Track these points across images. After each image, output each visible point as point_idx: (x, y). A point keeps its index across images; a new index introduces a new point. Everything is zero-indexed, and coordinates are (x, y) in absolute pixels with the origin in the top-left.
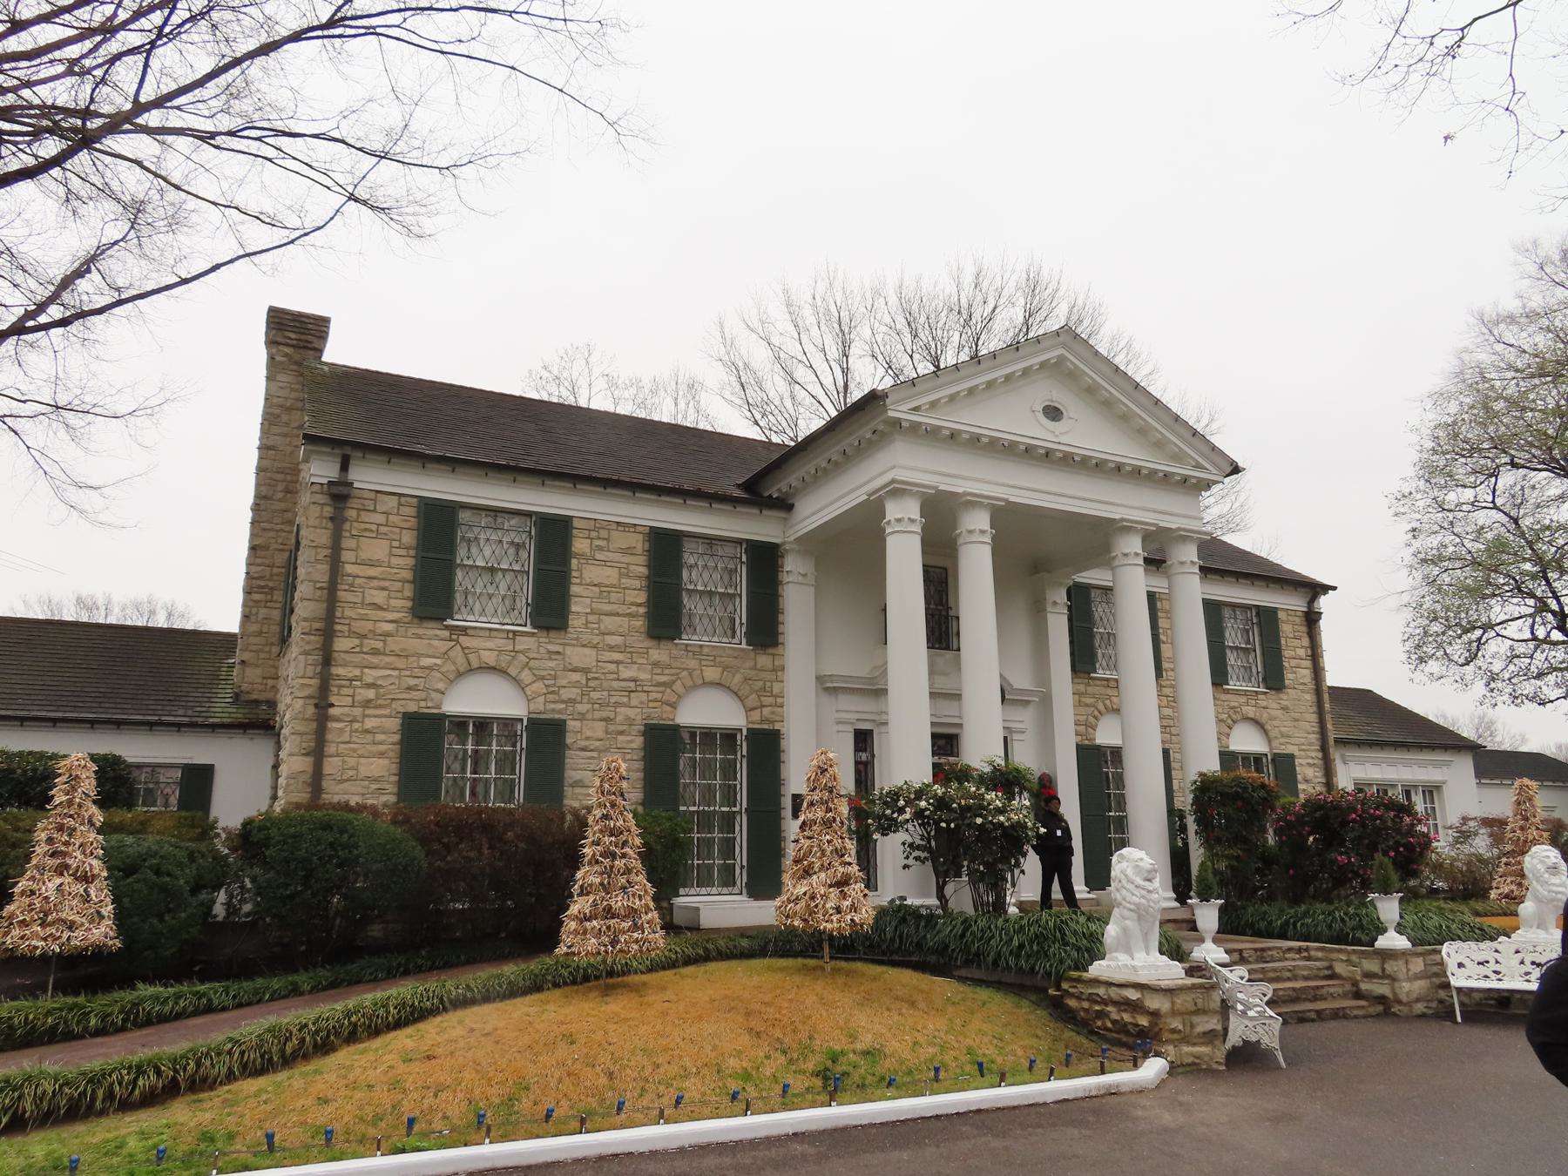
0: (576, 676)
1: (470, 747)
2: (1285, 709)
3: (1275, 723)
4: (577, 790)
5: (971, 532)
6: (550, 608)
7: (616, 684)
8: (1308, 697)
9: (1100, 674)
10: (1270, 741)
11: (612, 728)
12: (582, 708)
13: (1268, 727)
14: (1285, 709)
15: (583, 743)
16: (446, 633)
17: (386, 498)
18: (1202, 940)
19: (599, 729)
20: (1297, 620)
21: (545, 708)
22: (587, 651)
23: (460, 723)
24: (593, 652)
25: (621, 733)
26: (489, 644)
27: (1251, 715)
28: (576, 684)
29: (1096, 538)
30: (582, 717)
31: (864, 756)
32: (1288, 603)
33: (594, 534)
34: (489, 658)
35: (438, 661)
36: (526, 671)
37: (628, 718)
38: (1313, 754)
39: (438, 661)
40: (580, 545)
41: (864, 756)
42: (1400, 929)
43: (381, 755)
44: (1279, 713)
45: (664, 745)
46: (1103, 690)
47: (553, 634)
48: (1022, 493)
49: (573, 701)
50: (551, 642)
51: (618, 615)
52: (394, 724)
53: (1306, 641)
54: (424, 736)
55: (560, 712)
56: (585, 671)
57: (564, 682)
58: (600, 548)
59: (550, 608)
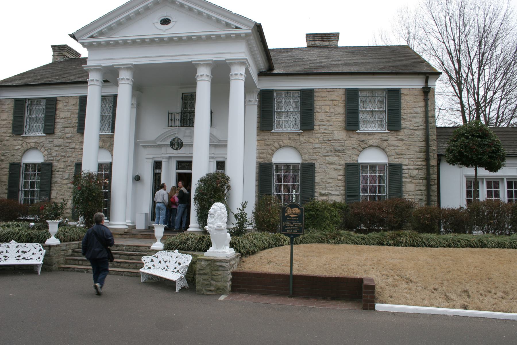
0: (57, 149)
1: (283, 174)
2: (402, 140)
3: (392, 148)
4: (56, 184)
5: (236, 74)
6: (307, 122)
7: (68, 150)
8: (419, 133)
9: (275, 130)
10: (388, 156)
11: (67, 164)
12: (58, 158)
13: (387, 150)
14: (402, 140)
15: (57, 170)
16: (21, 139)
17: (7, 100)
18: (156, 241)
19: (62, 165)
20: (417, 93)
21: (307, 159)
22: (60, 140)
23: (364, 167)
24: (62, 140)
25: (69, 166)
26: (33, 141)
27: (375, 144)
28: (57, 151)
29: (187, 73)
30: (58, 161)
31: (158, 171)
32: (409, 85)
33: (64, 101)
34: (33, 145)
35: (20, 147)
36: (43, 148)
37: (71, 161)
38: (419, 163)
39: (20, 147)
40: (60, 106)
41: (158, 171)
42: (57, 236)
43: (6, 175)
44: (396, 143)
45: (352, 171)
46: (279, 137)
47: (51, 136)
48: (170, 58)
49: (56, 156)
50: (50, 139)
51: (69, 127)
52: (8, 166)
53: (422, 104)
54: (352, 171)
55: (52, 160)
56: (59, 146)
57: (53, 151)
58: (66, 106)
59: (307, 122)
